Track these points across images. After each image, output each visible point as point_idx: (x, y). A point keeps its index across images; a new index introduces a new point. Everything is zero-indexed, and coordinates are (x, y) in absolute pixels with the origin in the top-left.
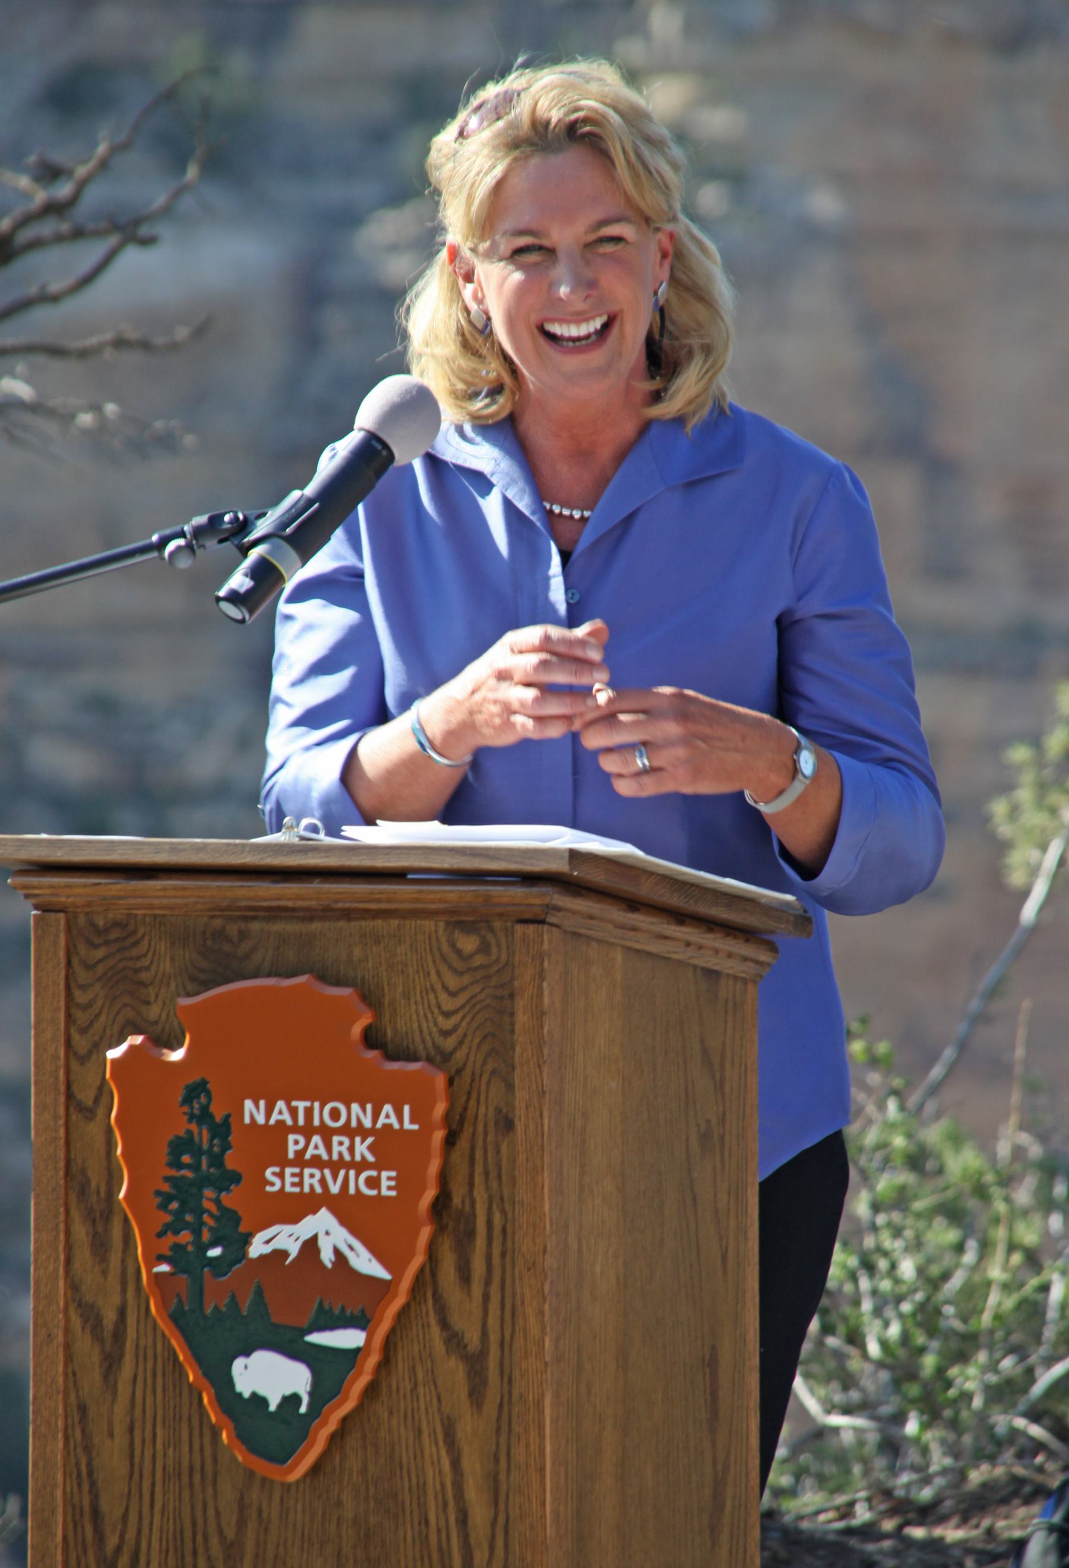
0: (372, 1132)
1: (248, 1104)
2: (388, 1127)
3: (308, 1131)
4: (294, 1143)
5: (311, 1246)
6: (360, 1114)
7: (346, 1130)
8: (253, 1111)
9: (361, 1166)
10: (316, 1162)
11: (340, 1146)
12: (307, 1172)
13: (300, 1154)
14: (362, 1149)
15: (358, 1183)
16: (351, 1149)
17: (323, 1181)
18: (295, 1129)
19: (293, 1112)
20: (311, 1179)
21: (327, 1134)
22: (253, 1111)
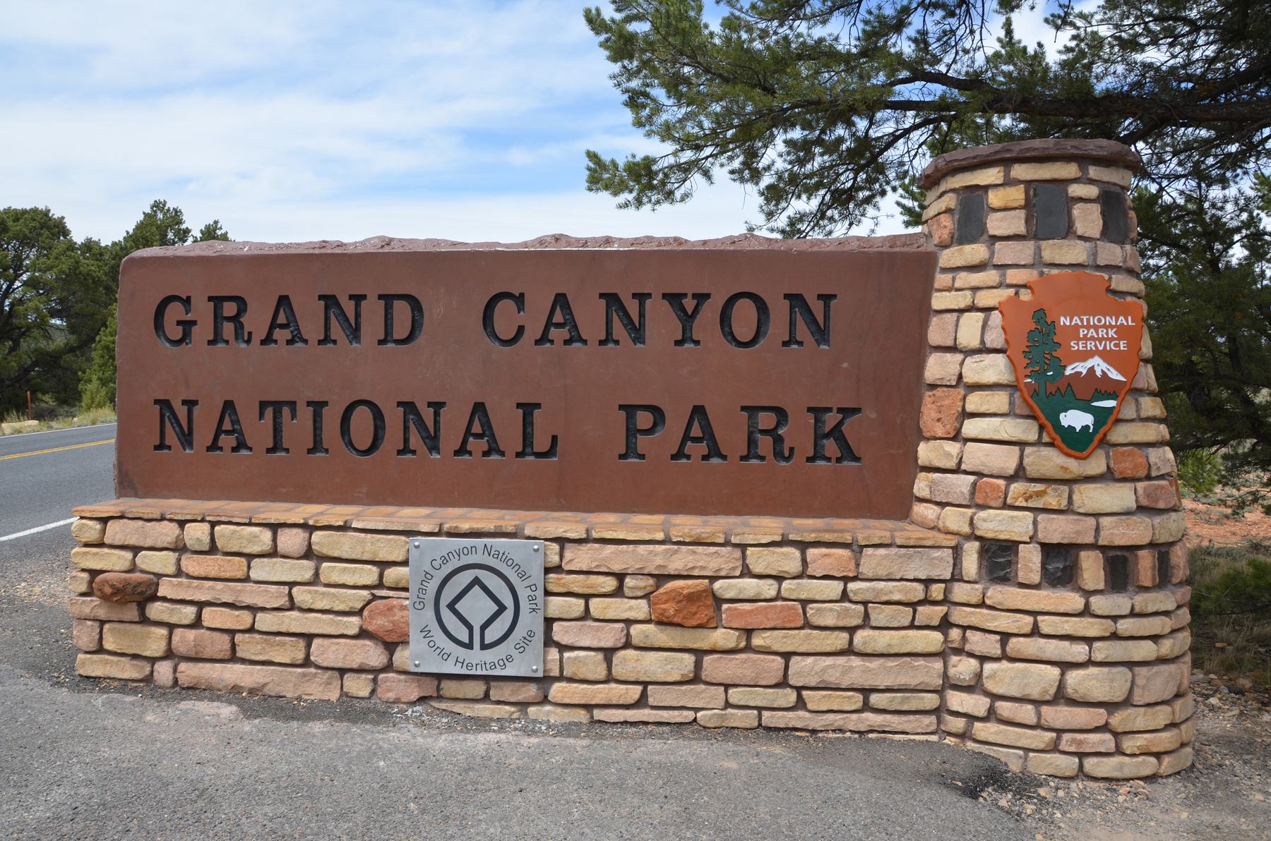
1: (1062, 319)
3: (1088, 327)
5: (1092, 370)
7: (1105, 326)
8: (1065, 321)
9: (1112, 339)
10: (1092, 338)
11: (1102, 332)
14: (1111, 333)
15: (1110, 346)
18: (1083, 326)
19: (1082, 320)
20: (1090, 345)
21: (1096, 328)
22: (1065, 321)
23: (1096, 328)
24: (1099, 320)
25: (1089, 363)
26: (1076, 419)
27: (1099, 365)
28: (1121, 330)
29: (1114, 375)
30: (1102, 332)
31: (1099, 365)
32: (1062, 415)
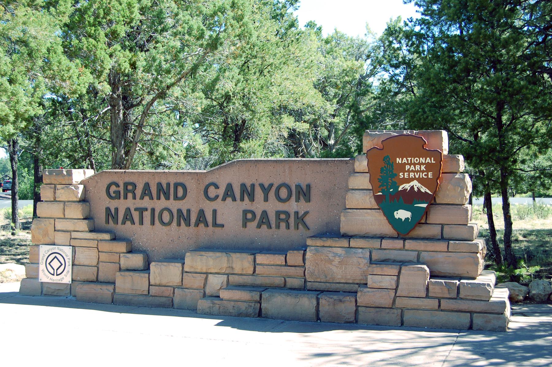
0: (425, 164)
1: (398, 159)
2: (428, 162)
3: (410, 165)
4: (407, 167)
5: (412, 187)
6: (422, 160)
8: (399, 160)
9: (423, 172)
10: (412, 171)
11: (418, 167)
12: (411, 173)
13: (409, 169)
14: (423, 168)
15: (423, 175)
16: (420, 168)
17: (414, 175)
18: (408, 164)
19: (408, 160)
20: (412, 175)
22: (399, 160)
23: (415, 164)
24: (417, 160)
25: (412, 184)
26: (402, 214)
27: (416, 184)
28: (428, 166)
29: (423, 189)
30: (418, 167)
31: (416, 184)
32: (395, 213)
